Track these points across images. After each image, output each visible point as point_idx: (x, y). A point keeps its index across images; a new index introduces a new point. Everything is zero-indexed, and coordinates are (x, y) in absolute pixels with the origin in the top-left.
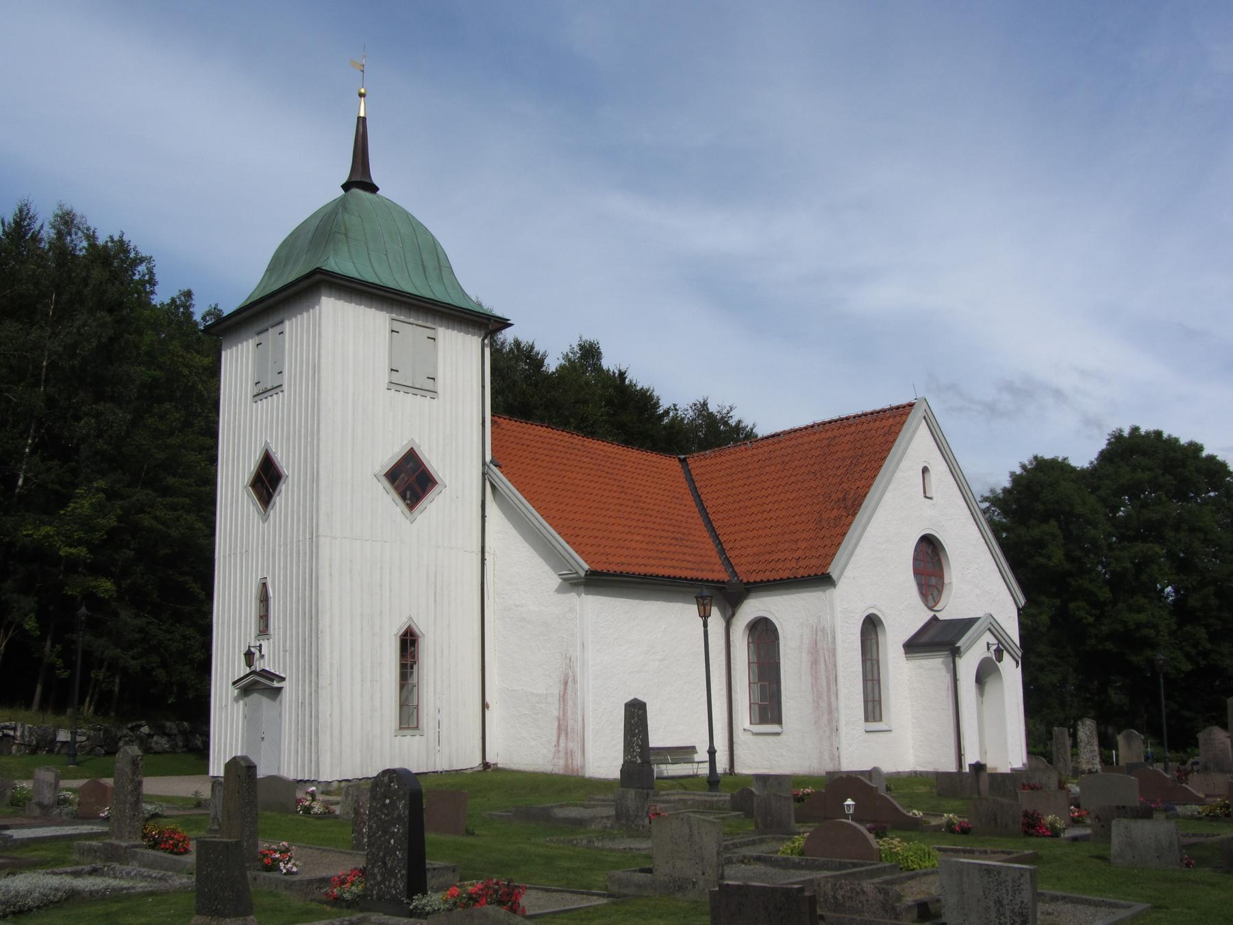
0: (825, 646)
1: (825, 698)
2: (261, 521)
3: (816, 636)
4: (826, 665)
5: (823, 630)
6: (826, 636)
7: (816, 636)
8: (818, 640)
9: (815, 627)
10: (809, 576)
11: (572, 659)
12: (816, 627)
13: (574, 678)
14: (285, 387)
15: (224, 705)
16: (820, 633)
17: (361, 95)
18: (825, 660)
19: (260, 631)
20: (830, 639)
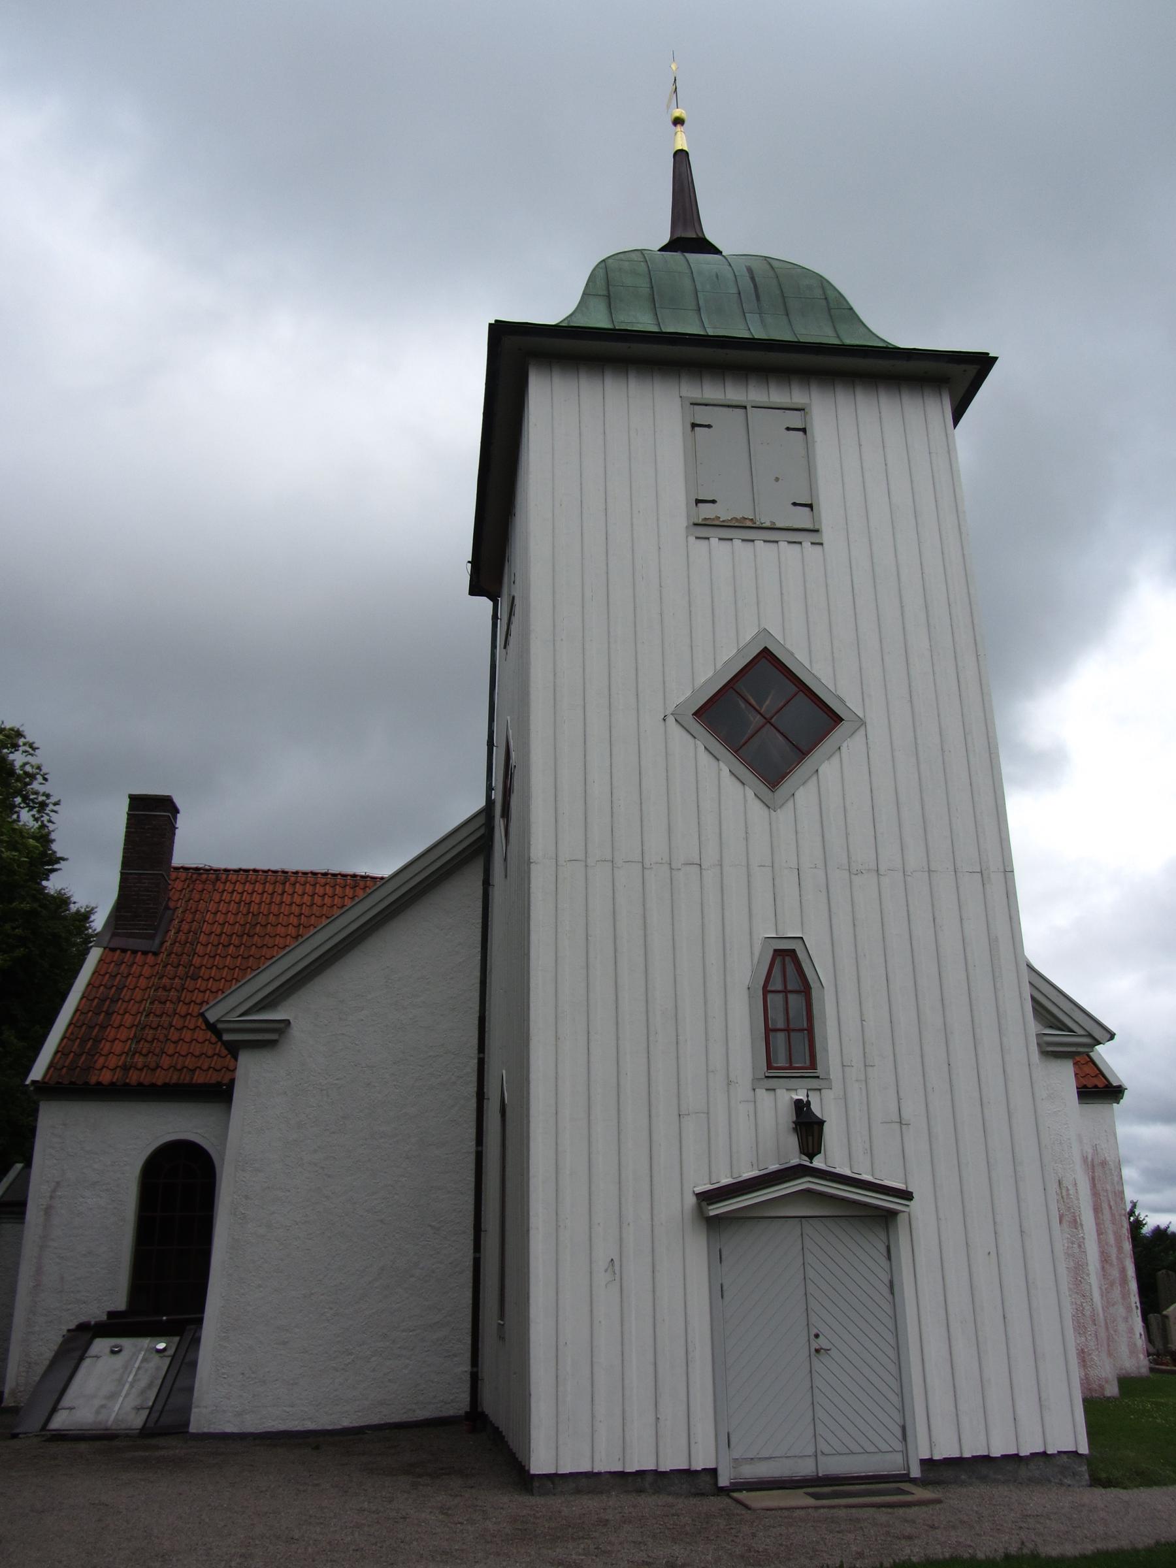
0: (1109, 1187)
1: (1115, 1261)
2: (756, 809)
3: (1093, 1172)
4: (1113, 1215)
5: (1104, 1164)
6: (1107, 1172)
7: (1093, 1172)
8: (1097, 1178)
9: (1090, 1159)
10: (1096, 1087)
11: (1065, 1183)
12: (1093, 1160)
13: (1075, 1221)
14: (827, 535)
15: (601, 1263)
16: (1099, 1172)
17: (678, 121)
18: (1110, 1207)
19: (769, 1066)
20: (1116, 1179)
